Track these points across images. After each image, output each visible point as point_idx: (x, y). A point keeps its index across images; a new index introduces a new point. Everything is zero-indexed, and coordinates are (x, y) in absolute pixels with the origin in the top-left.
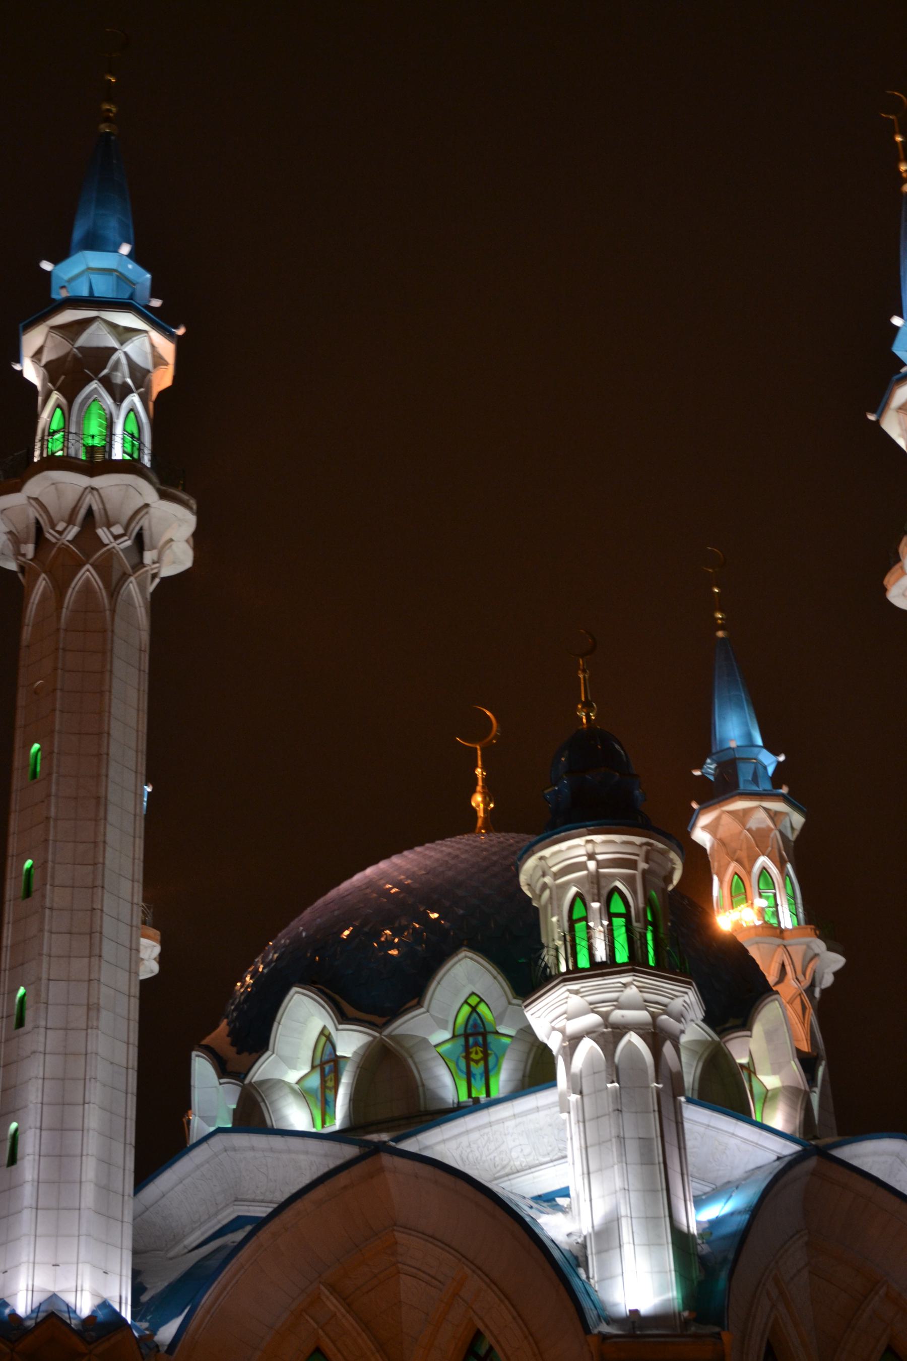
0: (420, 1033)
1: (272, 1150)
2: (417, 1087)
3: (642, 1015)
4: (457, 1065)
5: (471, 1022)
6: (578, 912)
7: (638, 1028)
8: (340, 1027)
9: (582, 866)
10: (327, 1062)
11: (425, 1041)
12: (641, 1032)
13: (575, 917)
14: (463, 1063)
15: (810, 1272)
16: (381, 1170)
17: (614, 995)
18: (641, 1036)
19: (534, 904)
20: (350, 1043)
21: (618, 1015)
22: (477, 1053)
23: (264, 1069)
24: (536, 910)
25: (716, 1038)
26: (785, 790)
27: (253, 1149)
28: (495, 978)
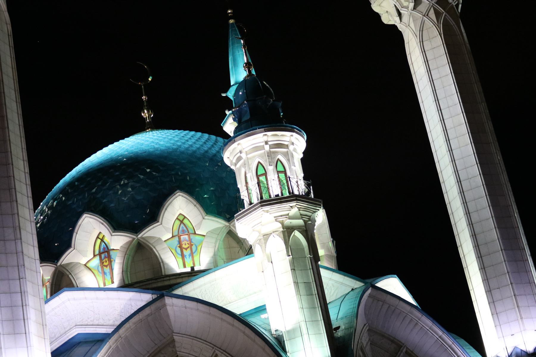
0: (157, 236)
2: (160, 263)
3: (300, 222)
4: (176, 251)
5: (181, 229)
7: (298, 228)
8: (114, 234)
9: (263, 148)
11: (160, 239)
12: (300, 230)
13: (259, 174)
14: (179, 250)
16: (165, 305)
17: (287, 213)
18: (300, 232)
19: (233, 167)
20: (118, 241)
21: (288, 222)
22: (185, 245)
23: (68, 258)
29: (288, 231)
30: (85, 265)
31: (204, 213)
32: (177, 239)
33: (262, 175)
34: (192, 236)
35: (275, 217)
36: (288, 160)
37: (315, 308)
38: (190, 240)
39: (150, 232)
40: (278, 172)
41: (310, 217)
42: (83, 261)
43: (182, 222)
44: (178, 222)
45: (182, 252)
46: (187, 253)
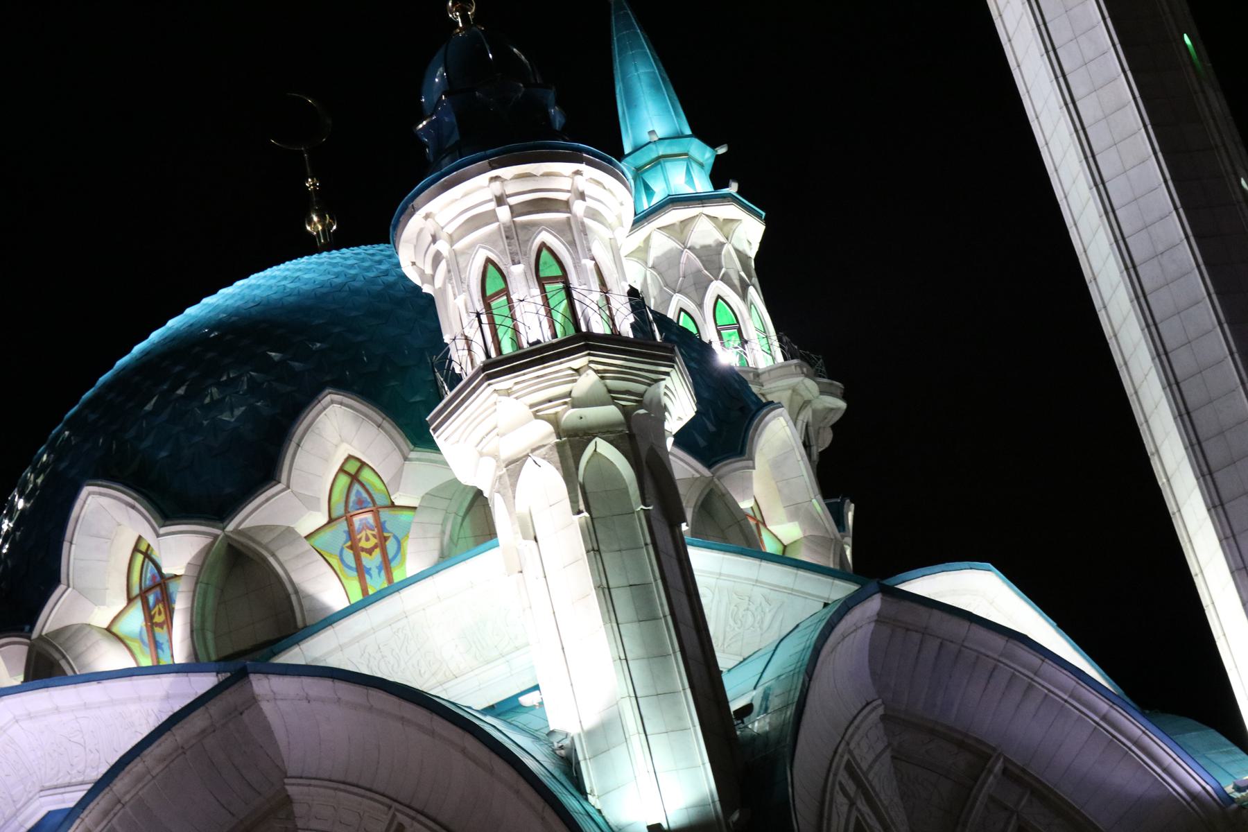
0: (282, 521)
1: (86, 706)
2: (288, 597)
3: (610, 413)
4: (342, 560)
5: (353, 498)
6: (494, 285)
8: (162, 531)
9: (491, 217)
10: (149, 590)
11: (290, 531)
12: (611, 436)
13: (489, 293)
14: (349, 556)
15: (893, 757)
16: (253, 700)
17: (564, 389)
18: (611, 442)
19: (426, 289)
20: (180, 550)
21: (570, 416)
22: (367, 539)
24: (430, 299)
25: (706, 472)
26: (733, 188)
27: (57, 710)
28: (379, 426)
29: (572, 442)
30: (108, 630)
31: (405, 444)
32: (342, 526)
33: (497, 294)
34: (385, 515)
35: (531, 406)
36: (572, 244)
37: (665, 656)
38: (381, 527)
39: (257, 515)
40: (542, 282)
41: (641, 395)
42: (101, 617)
43: (354, 478)
44: (344, 480)
45: (358, 559)
46: (372, 561)
